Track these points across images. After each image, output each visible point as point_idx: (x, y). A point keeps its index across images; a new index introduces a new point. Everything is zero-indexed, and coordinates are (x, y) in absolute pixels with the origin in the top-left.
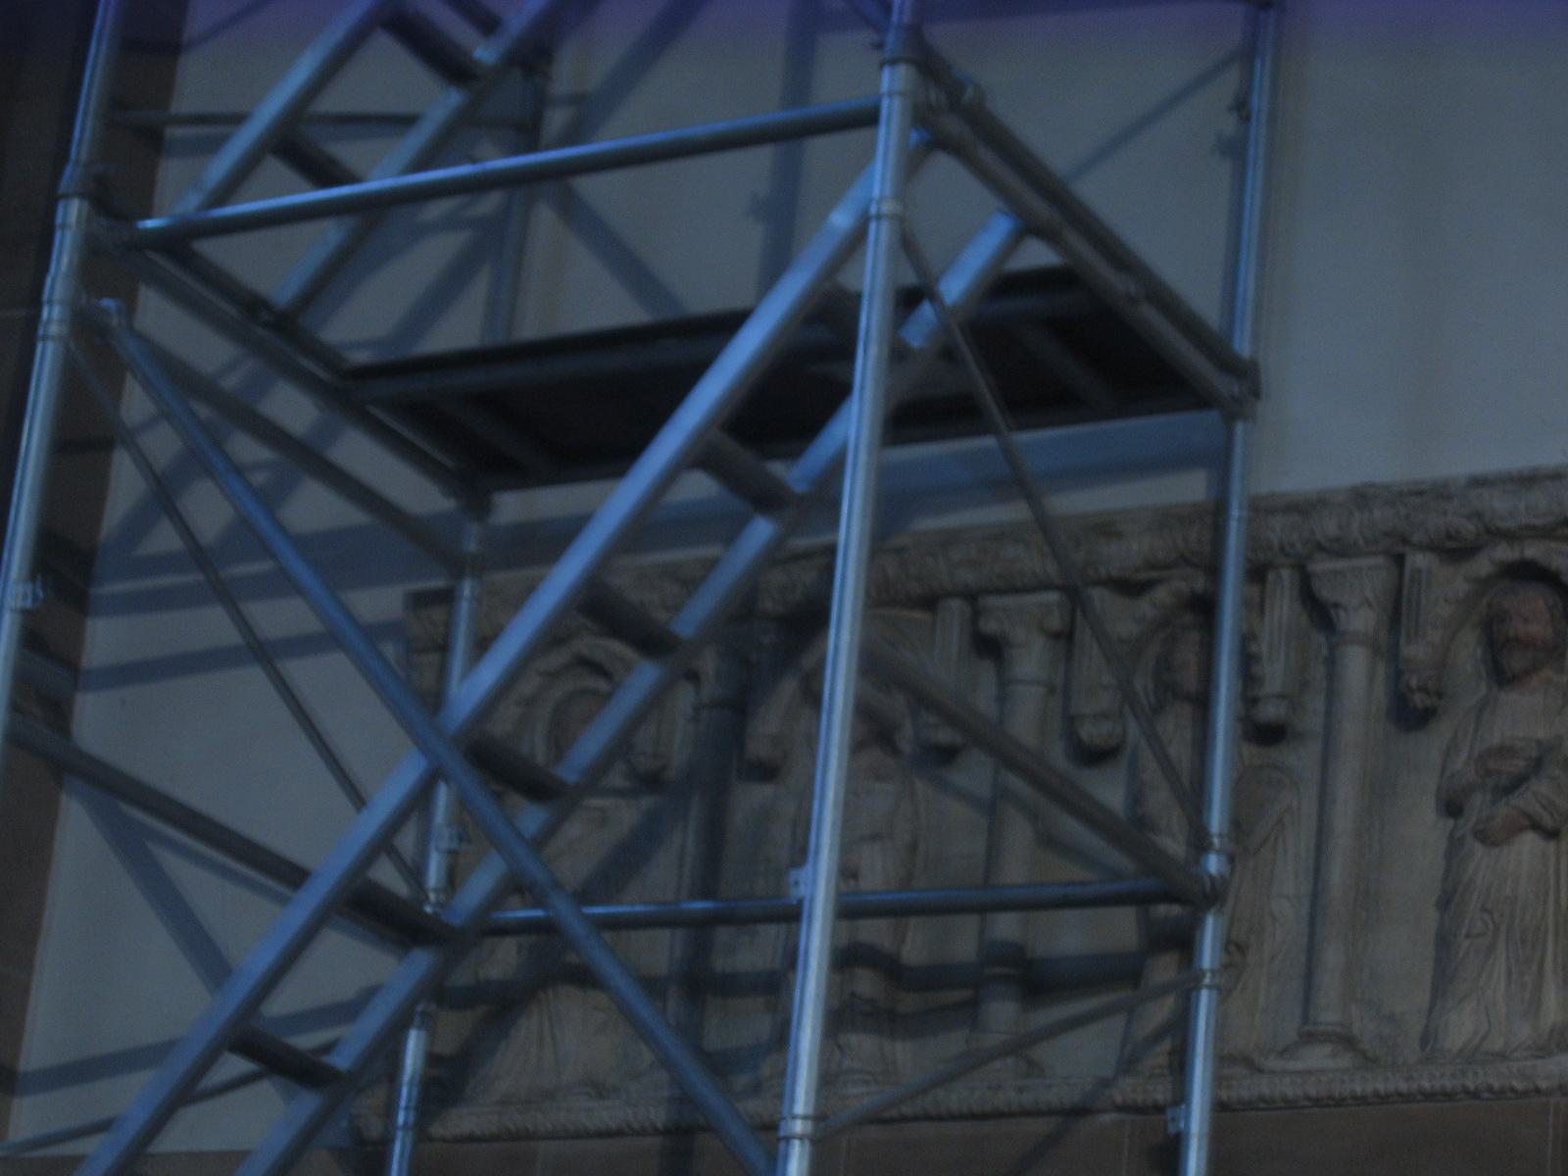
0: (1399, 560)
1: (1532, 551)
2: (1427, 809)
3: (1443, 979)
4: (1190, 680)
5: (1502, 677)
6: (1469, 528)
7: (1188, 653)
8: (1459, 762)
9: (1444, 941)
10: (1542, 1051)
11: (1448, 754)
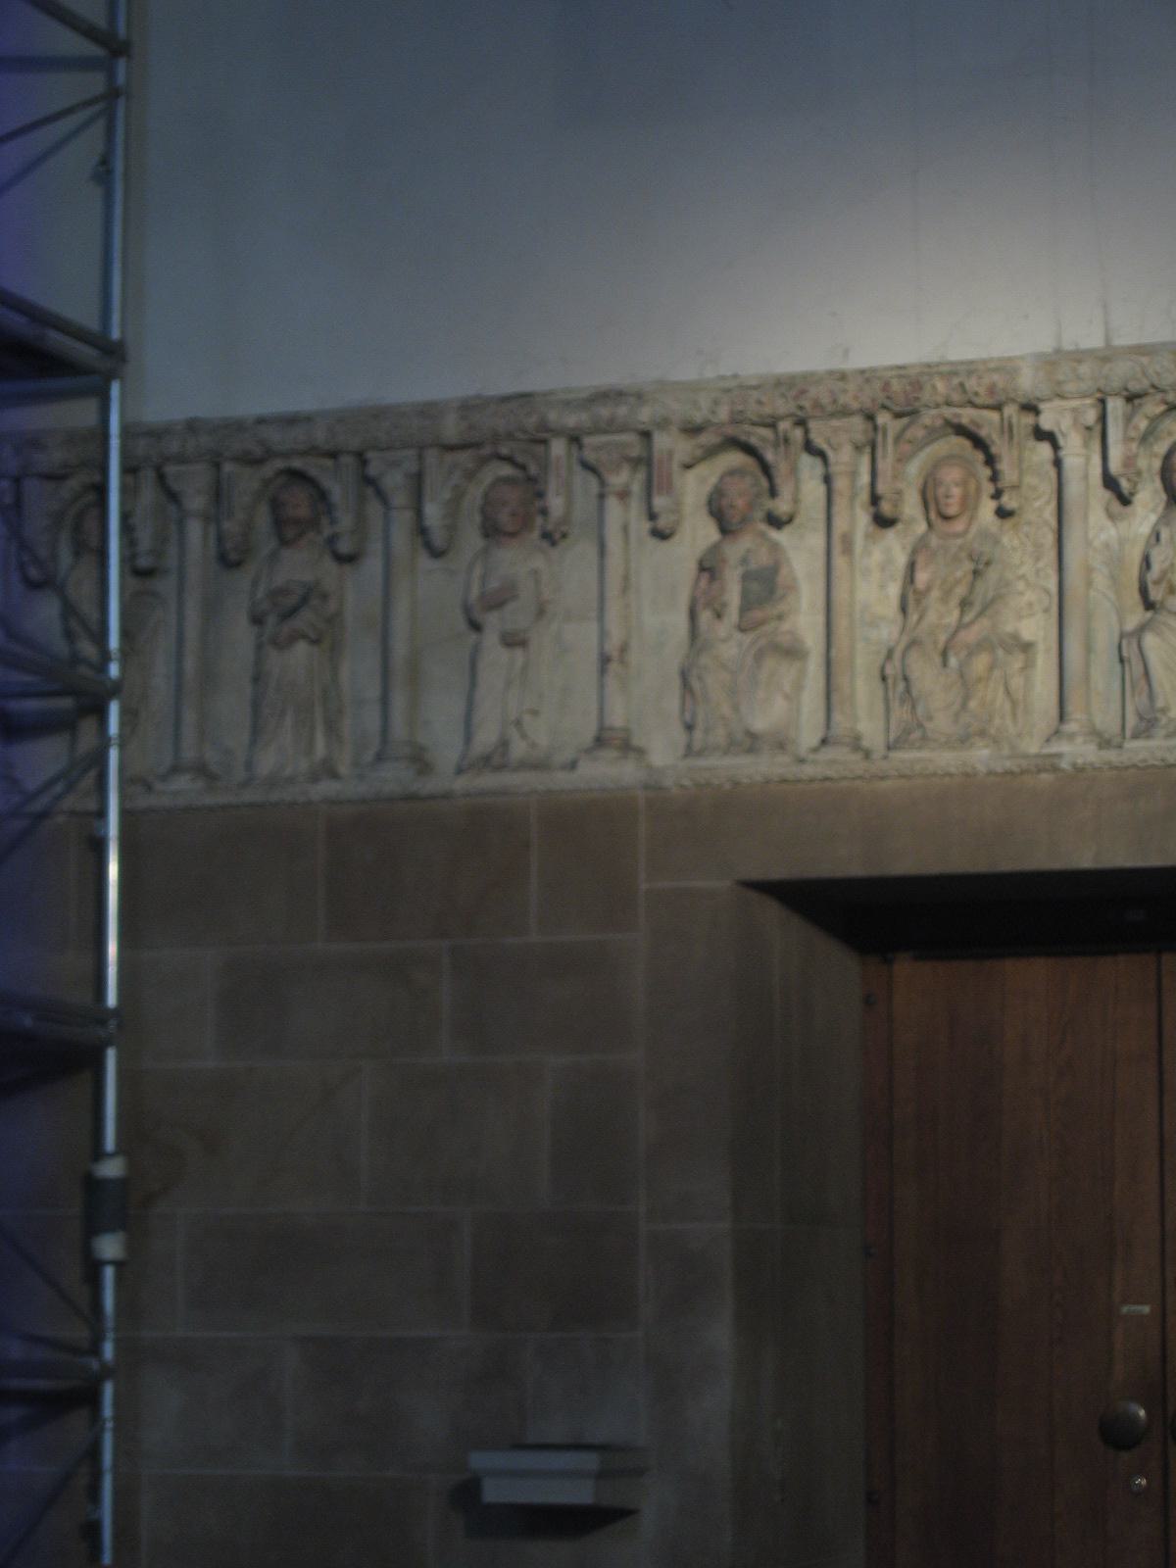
0: (217, 466)
1: (297, 463)
2: (243, 620)
3: (256, 731)
4: (94, 542)
5: (284, 542)
6: (258, 451)
7: (91, 524)
8: (260, 594)
9: (256, 705)
10: (314, 778)
11: (255, 583)
